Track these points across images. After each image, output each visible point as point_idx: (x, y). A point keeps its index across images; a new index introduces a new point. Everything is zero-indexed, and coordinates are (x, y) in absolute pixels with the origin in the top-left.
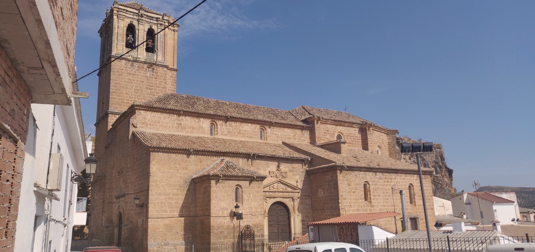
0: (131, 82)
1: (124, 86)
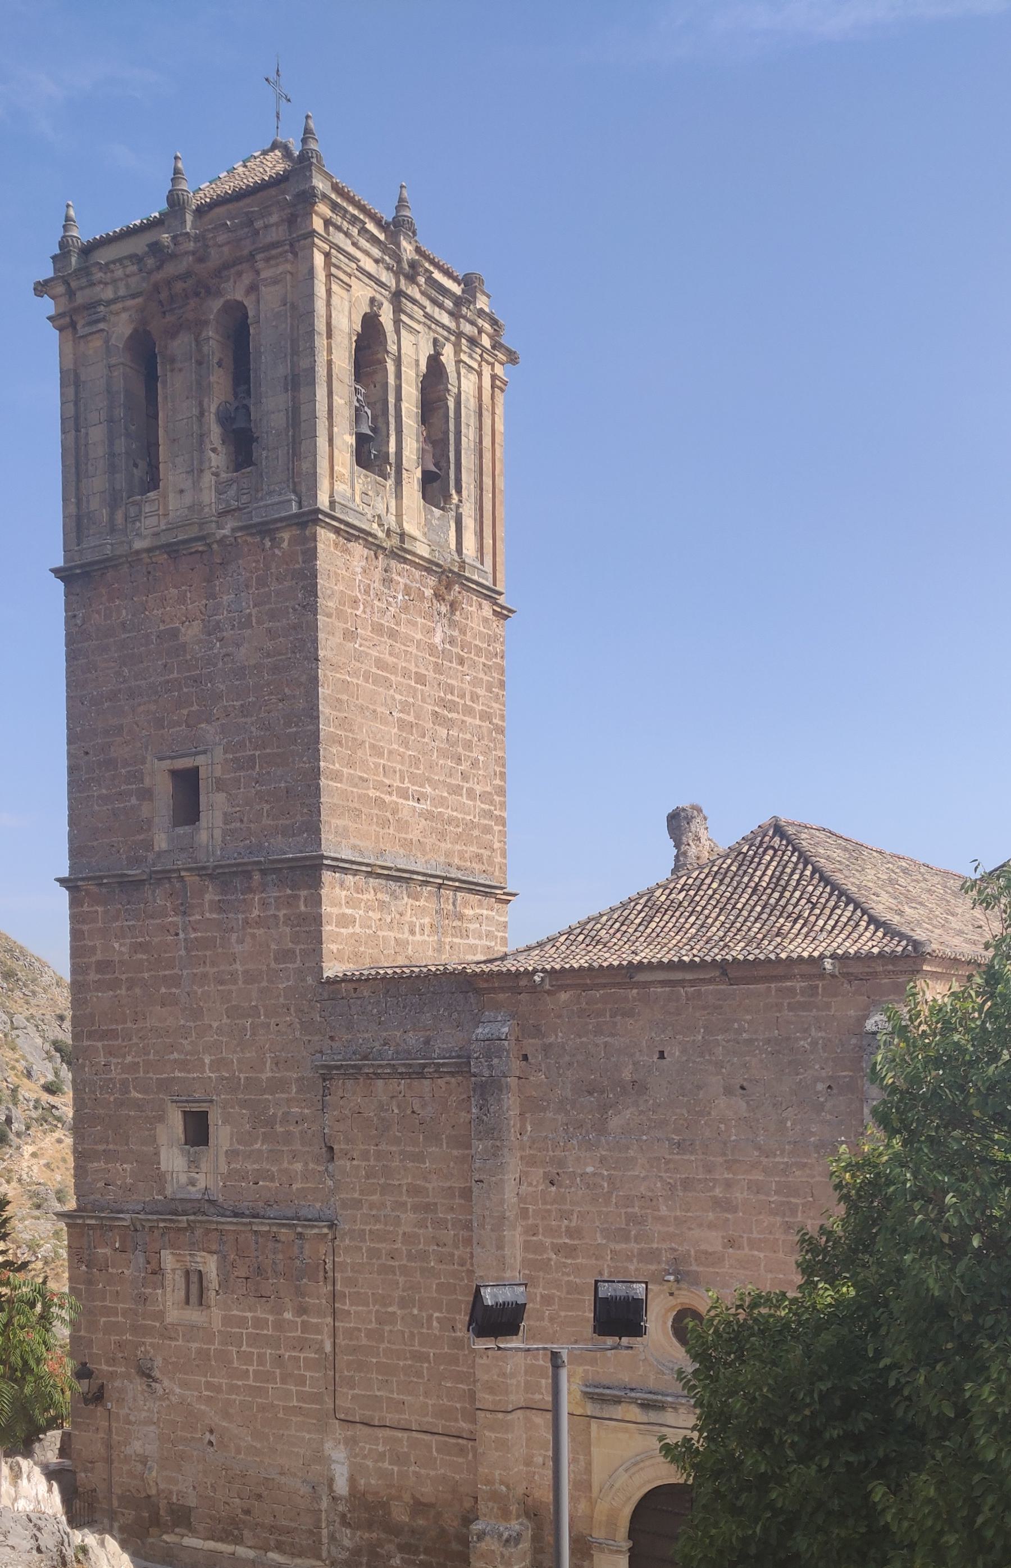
0: (386, 679)
1: (365, 704)
